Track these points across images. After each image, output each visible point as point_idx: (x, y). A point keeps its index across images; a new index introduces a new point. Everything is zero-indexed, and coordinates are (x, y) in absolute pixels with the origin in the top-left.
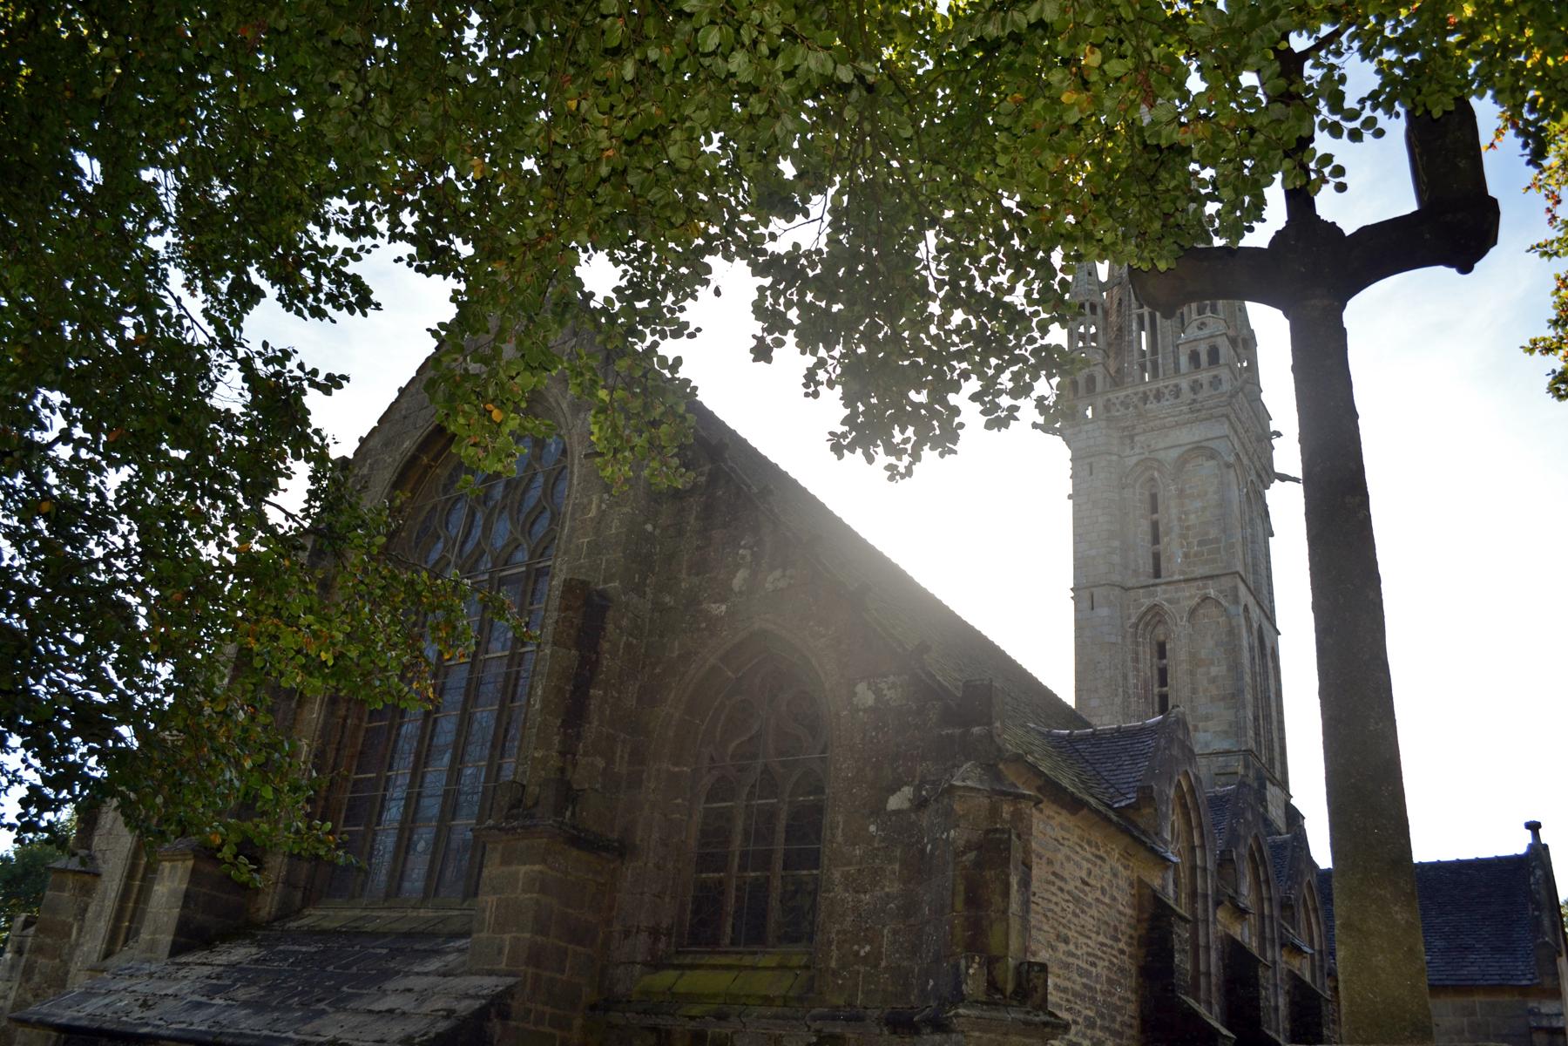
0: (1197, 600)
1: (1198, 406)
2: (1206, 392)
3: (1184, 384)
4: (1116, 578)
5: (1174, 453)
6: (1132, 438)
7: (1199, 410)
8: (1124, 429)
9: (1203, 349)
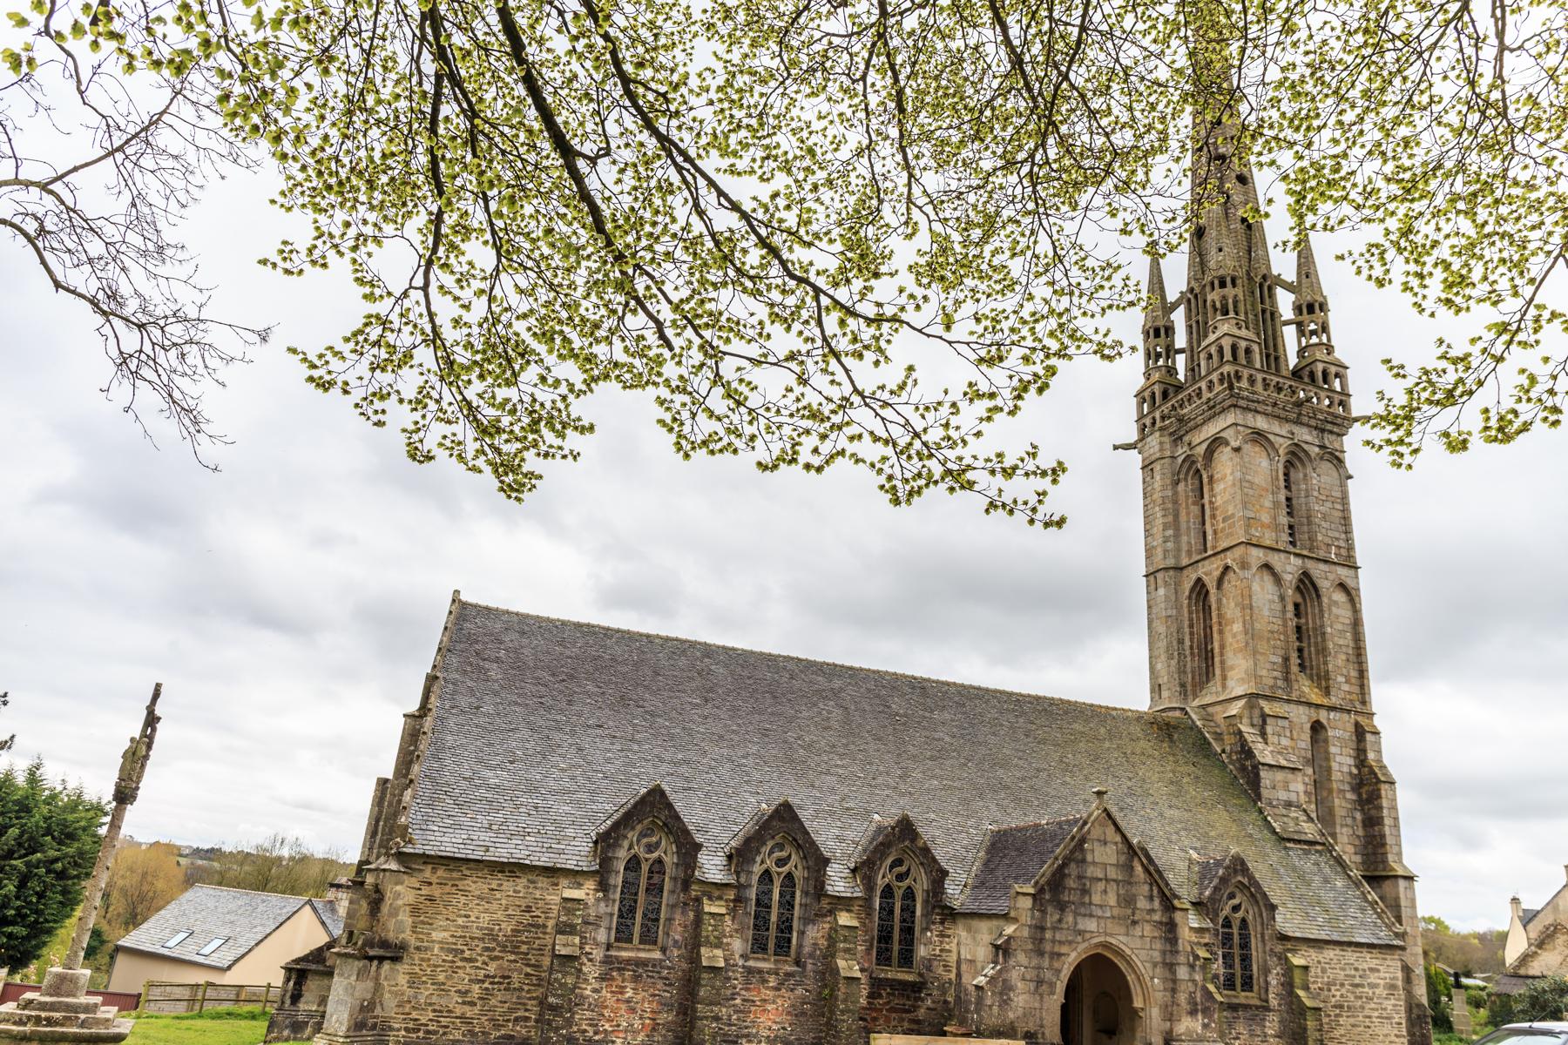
0: (1221, 569)
1: (1212, 403)
2: (1218, 388)
3: (1203, 385)
4: (1171, 562)
5: (1204, 446)
6: (1181, 438)
7: (1214, 407)
8: (1171, 434)
9: (1213, 350)
